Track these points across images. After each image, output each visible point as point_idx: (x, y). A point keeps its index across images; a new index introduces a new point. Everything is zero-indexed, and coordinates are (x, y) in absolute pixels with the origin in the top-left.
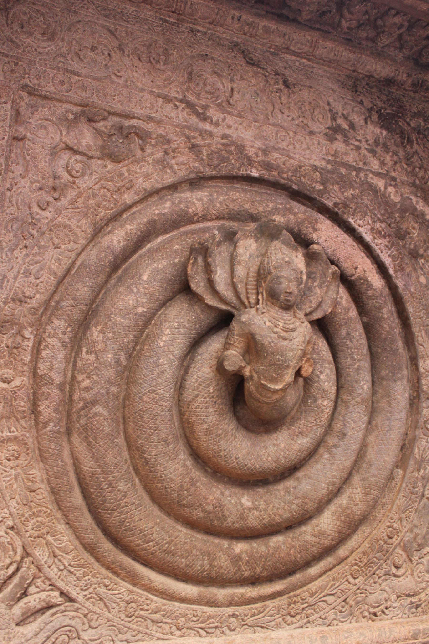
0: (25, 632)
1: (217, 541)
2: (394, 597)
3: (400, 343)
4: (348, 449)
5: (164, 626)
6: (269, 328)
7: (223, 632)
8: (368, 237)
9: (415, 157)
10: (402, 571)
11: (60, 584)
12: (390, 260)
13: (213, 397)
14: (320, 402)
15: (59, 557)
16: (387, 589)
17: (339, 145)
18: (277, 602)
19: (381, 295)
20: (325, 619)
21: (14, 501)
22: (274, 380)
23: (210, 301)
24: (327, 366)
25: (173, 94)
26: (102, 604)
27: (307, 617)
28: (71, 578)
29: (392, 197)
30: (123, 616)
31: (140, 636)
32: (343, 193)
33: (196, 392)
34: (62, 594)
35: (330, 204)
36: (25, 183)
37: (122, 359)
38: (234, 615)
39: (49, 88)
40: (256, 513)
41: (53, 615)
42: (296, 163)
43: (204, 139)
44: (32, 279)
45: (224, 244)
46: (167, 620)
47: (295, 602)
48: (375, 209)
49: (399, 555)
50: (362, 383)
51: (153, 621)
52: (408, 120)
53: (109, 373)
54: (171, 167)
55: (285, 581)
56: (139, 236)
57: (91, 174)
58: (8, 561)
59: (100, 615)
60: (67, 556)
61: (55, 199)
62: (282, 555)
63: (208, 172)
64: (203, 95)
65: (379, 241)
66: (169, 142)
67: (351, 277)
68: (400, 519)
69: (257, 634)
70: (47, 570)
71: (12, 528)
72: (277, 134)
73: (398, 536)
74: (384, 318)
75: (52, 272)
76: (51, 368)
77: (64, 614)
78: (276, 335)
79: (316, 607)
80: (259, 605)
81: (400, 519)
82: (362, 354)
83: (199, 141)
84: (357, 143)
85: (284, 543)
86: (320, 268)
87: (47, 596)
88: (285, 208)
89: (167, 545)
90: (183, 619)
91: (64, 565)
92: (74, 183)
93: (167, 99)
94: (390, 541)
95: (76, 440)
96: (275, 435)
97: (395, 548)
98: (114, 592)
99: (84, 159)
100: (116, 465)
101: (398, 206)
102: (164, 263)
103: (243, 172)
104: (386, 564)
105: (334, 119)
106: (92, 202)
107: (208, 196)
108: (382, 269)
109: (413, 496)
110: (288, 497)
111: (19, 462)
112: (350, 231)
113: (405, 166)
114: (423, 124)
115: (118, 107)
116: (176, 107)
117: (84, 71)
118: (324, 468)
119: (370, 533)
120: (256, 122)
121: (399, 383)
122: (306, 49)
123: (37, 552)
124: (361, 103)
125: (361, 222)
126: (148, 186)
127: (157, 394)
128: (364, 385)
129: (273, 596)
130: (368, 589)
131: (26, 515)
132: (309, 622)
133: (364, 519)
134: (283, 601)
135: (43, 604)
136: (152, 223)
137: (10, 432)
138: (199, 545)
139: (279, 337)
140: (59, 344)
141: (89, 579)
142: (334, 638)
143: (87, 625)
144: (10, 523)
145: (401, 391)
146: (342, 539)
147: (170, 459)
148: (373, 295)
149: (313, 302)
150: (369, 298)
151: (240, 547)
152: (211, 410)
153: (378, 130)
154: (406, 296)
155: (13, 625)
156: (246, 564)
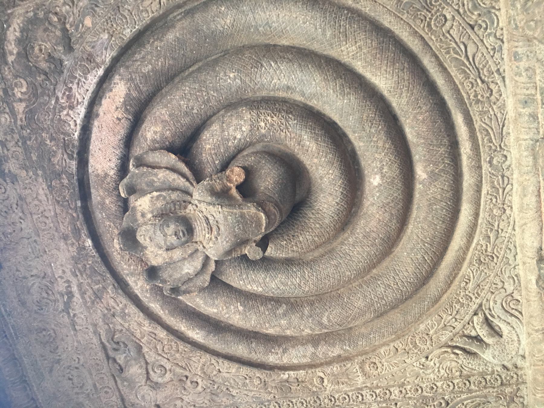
3: (170, 36)
4: (302, 81)
8: (82, 110)
11: (467, 318)
12: (90, 77)
13: (290, 240)
14: (263, 131)
15: (446, 323)
18: (476, 118)
20: (494, 49)
21: (406, 360)
25: (66, 320)
27: (493, 73)
28: (462, 311)
29: (24, 90)
31: (511, 246)
33: (290, 252)
35: (74, 165)
38: (490, 162)
45: (162, 276)
46: (496, 226)
48: (49, 108)
51: (497, 238)
54: (123, 310)
55: (453, 112)
56: (186, 319)
57: (157, 361)
58: (452, 356)
60: (444, 318)
66: (104, 315)
67: (129, 119)
71: (427, 358)
72: (43, 230)
74: (153, 70)
75: (237, 371)
76: (305, 356)
77: (492, 309)
78: (218, 238)
83: (90, 293)
85: (413, 128)
86: (139, 181)
88: (102, 208)
89: (426, 245)
90: (495, 211)
91: (452, 319)
93: (73, 324)
96: (308, 167)
98: (472, 276)
99: (150, 368)
102: (198, 300)
103: (94, 252)
107: (130, 278)
112: (86, 130)
115: (101, 355)
116: (75, 315)
117: (90, 382)
118: (328, 103)
120: (46, 251)
123: (444, 339)
125: (72, 123)
126: (146, 322)
129: (469, 121)
132: (498, 70)
134: (474, 111)
136: (172, 313)
139: (219, 234)
140: (286, 355)
141: (462, 298)
142: (516, 44)
144: (423, 360)
148: (136, 88)
150: (140, 92)
151: (421, 172)
152: (301, 239)
154: (117, 44)
156: (438, 165)
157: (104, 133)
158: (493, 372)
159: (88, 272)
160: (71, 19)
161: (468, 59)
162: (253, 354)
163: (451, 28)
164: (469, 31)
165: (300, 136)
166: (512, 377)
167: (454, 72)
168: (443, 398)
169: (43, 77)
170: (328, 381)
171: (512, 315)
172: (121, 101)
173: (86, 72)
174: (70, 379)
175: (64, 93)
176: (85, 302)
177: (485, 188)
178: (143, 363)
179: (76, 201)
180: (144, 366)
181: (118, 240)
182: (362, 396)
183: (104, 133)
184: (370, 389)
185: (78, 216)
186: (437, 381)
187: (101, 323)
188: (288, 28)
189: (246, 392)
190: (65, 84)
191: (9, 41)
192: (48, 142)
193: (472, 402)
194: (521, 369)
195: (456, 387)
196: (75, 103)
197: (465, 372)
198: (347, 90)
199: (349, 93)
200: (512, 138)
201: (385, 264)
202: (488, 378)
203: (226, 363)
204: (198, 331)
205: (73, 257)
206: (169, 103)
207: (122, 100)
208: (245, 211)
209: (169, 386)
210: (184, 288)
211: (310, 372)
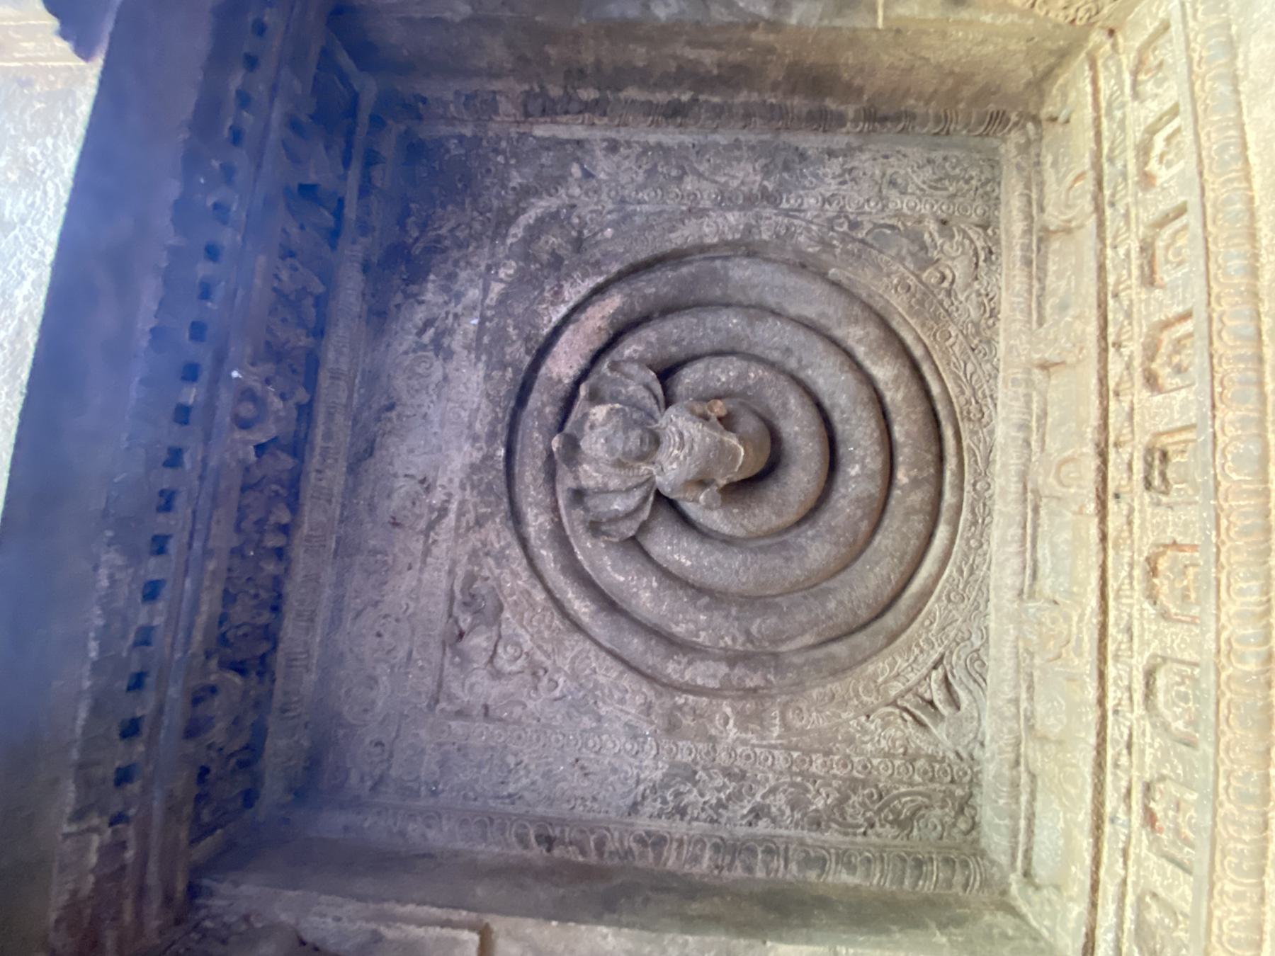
1: (893, 502)
2: (976, 285)
3: (685, 270)
6: (680, 465)
7: (991, 497)
8: (563, 310)
9: (458, 234)
10: (947, 272)
11: (924, 671)
14: (751, 382)
17: (457, 342)
23: (645, 514)
25: (420, 546)
26: (949, 628)
28: (921, 659)
29: (511, 272)
30: (962, 606)
31: (984, 589)
32: (514, 342)
35: (528, 359)
36: (531, 705)
38: (974, 485)
39: (429, 682)
40: (868, 460)
41: (953, 676)
42: (484, 401)
43: (469, 512)
44: (628, 696)
47: (969, 412)
49: (930, 276)
52: (411, 241)
53: (718, 618)
54: (503, 549)
57: (517, 635)
58: (899, 721)
59: (959, 630)
61: (546, 671)
62: (915, 429)
63: (505, 505)
64: (417, 511)
65: (566, 294)
68: (888, 275)
69: (997, 458)
71: (868, 717)
76: (714, 676)
81: (888, 275)
82: (697, 324)
83: (471, 517)
84: (451, 317)
85: (902, 425)
90: (972, 542)
92: (527, 654)
93: (427, 552)
94: (913, 289)
95: (783, 648)
96: (784, 435)
97: (921, 282)
99: (501, 644)
100: (811, 611)
101: (521, 264)
103: (501, 466)
105: (424, 347)
106: (546, 634)
108: (599, 291)
110: (854, 422)
111: (804, 709)
112: (557, 331)
113: (471, 249)
114: (413, 218)
115: (443, 607)
117: (407, 646)
119: (901, 315)
121: (731, 273)
122: (342, 383)
123: (893, 693)
124: (398, 306)
125: (546, 318)
126: (525, 575)
128: (733, 321)
131: (856, 703)
132: (991, 396)
133: (884, 324)
134: (965, 427)
135: (943, 687)
138: (896, 524)
144: (863, 719)
145: (741, 271)
146: (904, 352)
147: (806, 555)
151: (902, 476)
153: (430, 286)
154: (630, 259)
155: (960, 713)
158: (944, 757)
159: (483, 487)
162: (649, 655)
164: (970, 352)
166: (965, 773)
168: (876, 787)
169: (538, 266)
170: (735, 725)
171: (975, 681)
173: (585, 276)
174: (379, 635)
176: (457, 528)
178: (494, 634)
180: (495, 638)
186: (874, 757)
187: (465, 559)
189: (619, 714)
190: (558, 279)
192: (511, 329)
193: (912, 801)
197: (910, 751)
198: (846, 368)
200: (998, 466)
201: (840, 577)
202: (937, 766)
203: (609, 661)
205: (472, 466)
208: (726, 439)
209: (516, 679)
210: (604, 528)
211: (714, 702)
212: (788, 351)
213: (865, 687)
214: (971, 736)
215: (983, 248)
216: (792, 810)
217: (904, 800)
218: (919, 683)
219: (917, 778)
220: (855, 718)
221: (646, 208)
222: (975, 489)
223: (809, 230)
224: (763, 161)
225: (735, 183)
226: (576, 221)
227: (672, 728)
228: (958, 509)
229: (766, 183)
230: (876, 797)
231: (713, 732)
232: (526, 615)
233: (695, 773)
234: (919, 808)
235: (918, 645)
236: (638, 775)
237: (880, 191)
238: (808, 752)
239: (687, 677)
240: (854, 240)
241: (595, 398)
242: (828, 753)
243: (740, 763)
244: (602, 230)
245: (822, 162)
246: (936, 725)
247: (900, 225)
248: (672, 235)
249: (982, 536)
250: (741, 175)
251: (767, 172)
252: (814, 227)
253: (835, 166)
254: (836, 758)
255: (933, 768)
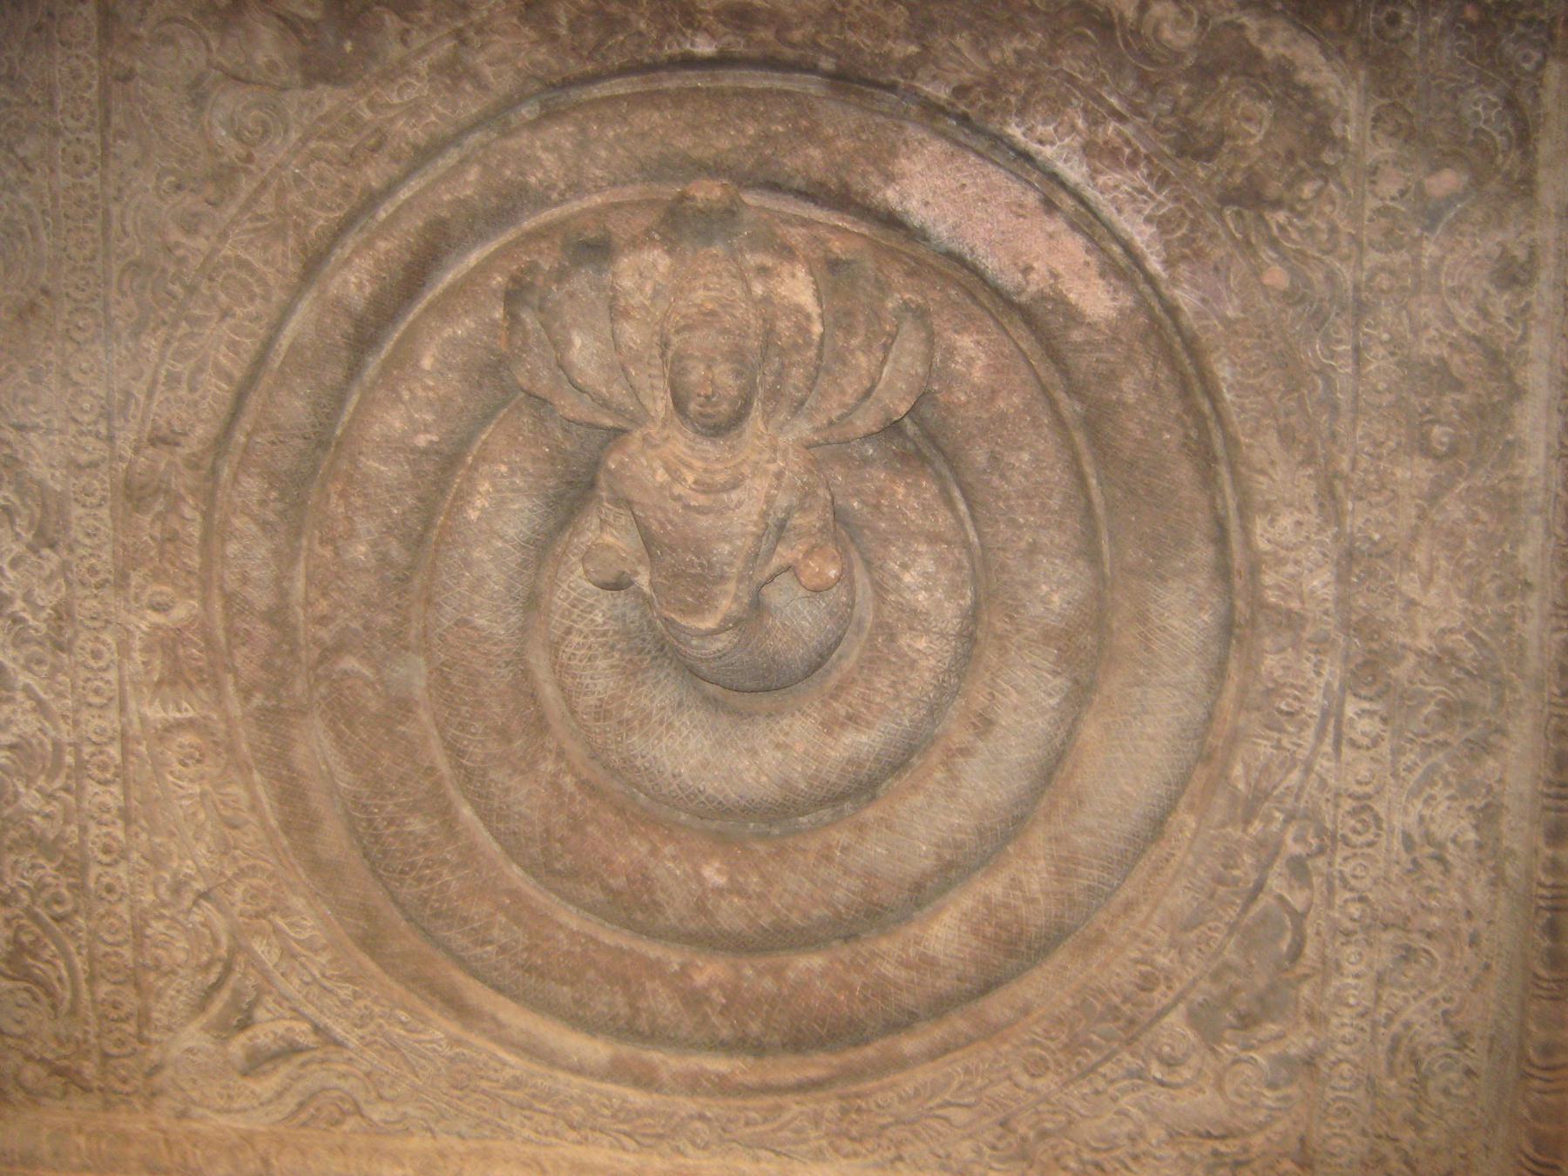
0: (258, 1089)
5: (537, 1117)
6: (662, 487)
7: (678, 1151)
8: (1074, 172)
10: (1187, 1074)
11: (310, 1010)
12: (1151, 230)
14: (904, 641)
16: (1134, 1111)
19: (1116, 339)
22: (697, 610)
24: (923, 548)
29: (1167, 34)
32: (984, 53)
33: (567, 623)
34: (317, 1029)
35: (942, 93)
37: (394, 553)
41: (303, 1065)
44: (183, 392)
50: (1044, 588)
51: (511, 1104)
54: (476, 77)
65: (1108, 178)
67: (1019, 294)
70: (280, 981)
73: (1169, 988)
74: (1124, 405)
79: (917, 1126)
80: (770, 1100)
85: (824, 974)
87: (289, 1029)
89: (525, 955)
101: (1189, 61)
103: (671, 49)
104: (1133, 1054)
109: (1221, 890)
121: (1175, 584)
123: (259, 946)
127: (475, 628)
129: (802, 1087)
130: (1076, 1105)
131: (229, 873)
132: (900, 1158)
137: (179, 710)
143: (374, 1094)
148: (1089, 343)
149: (850, 391)
150: (1078, 348)
152: (601, 664)
157: (1002, 217)
160: (1294, 235)
161: (940, 1106)
163: (1017, 1085)
164: (1001, 1115)
165: (869, 725)
167: (923, 1075)
168: (76, 911)
169: (1185, 101)
170: (157, 627)
171: (301, 1105)
172: (1071, 296)
173: (1163, 224)
175: (1128, 143)
177: (638, 1098)
179: (838, 57)
181: (719, 201)
182: (102, 707)
183: (1002, 217)
184: (124, 736)
185: (793, 45)
188: (1121, 755)
191: (1295, 40)
193: (60, 979)
194: (148, 1107)
195: (108, 949)
196: (1098, 164)
197: (152, 977)
199: (939, 857)
202: (131, 1028)
203: (250, 345)
204: (368, 290)
206: (1034, 419)
207: (1072, 297)
208: (731, 587)
212: (984, 724)
213: (263, 892)
214: (195, 1095)
215: (1245, 1150)
216: (12, 747)
217: (61, 963)
218: (283, 998)
219: (104, 989)
220: (199, 870)
221: (1345, 369)
222: (691, 1117)
223: (1290, 764)
224: (1469, 652)
225: (1412, 588)
226: (1307, 190)
227: (134, 494)
228: (645, 1079)
229: (1411, 659)
230: (58, 909)
231: (135, 578)
232: (332, 145)
233: (52, 545)
234: (50, 994)
235: (356, 996)
236: (35, 427)
237: (1386, 927)
238: (123, 776)
239: (237, 522)
240: (1264, 867)
241: (832, 272)
242: (126, 815)
243: (84, 640)
244: (1283, 258)
245: (1466, 790)
246: (205, 1029)
247: (1300, 970)
248: (1272, 440)
249: (593, 1129)
250: (1432, 598)
251: (1442, 660)
252: (1295, 777)
253: (1452, 823)
254: (120, 834)
255: (125, 1020)
